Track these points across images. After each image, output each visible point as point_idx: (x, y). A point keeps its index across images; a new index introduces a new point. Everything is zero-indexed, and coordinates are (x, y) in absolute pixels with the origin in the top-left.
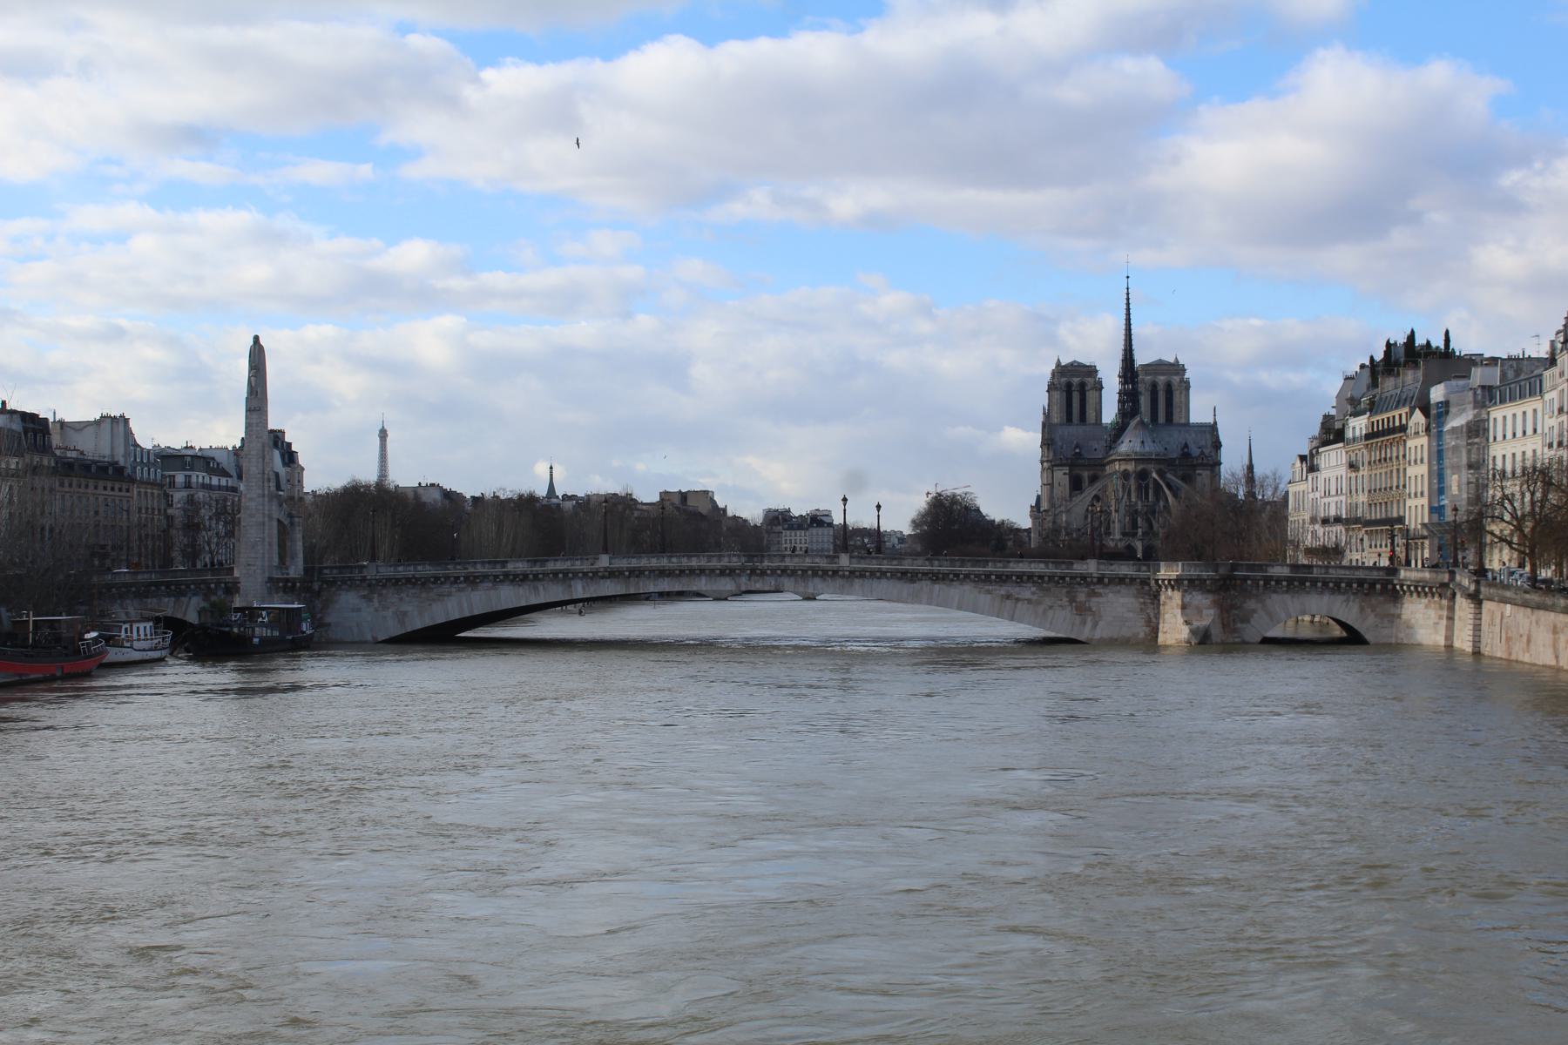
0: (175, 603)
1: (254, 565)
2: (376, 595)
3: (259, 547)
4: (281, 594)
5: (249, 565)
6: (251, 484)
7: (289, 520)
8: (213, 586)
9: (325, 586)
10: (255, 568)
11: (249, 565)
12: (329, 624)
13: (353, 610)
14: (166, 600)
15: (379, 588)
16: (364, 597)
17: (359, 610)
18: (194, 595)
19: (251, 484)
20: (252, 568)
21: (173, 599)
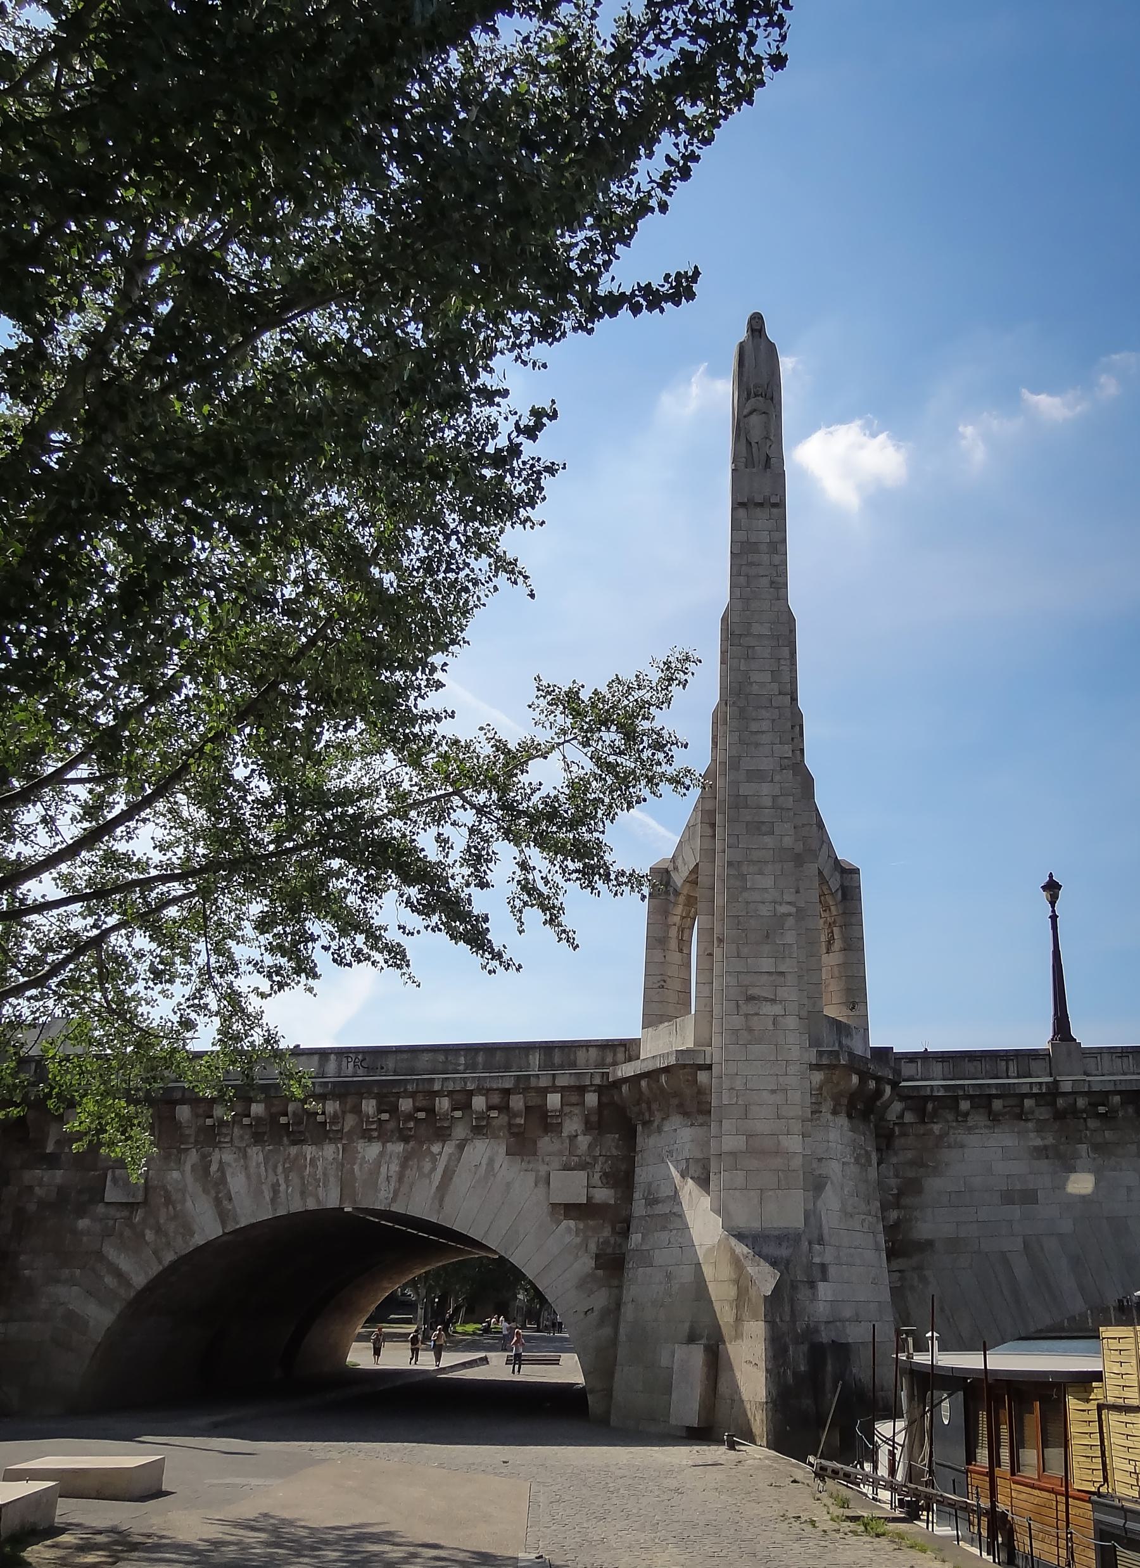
0: (404, 1165)
1: (773, 1001)
2: (1083, 1148)
3: (790, 938)
4: (843, 1121)
5: (750, 999)
6: (754, 727)
7: (837, 875)
8: (554, 1100)
9: (909, 1118)
10: (777, 1009)
11: (750, 999)
12: (930, 1243)
13: (1008, 1198)
14: (372, 1151)
15: (1093, 1124)
16: (1041, 1152)
17: (1029, 1197)
18: (479, 1130)
19: (754, 727)
20: (768, 1009)
21: (398, 1148)
